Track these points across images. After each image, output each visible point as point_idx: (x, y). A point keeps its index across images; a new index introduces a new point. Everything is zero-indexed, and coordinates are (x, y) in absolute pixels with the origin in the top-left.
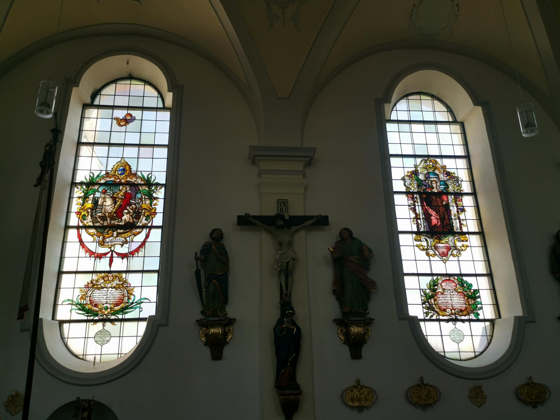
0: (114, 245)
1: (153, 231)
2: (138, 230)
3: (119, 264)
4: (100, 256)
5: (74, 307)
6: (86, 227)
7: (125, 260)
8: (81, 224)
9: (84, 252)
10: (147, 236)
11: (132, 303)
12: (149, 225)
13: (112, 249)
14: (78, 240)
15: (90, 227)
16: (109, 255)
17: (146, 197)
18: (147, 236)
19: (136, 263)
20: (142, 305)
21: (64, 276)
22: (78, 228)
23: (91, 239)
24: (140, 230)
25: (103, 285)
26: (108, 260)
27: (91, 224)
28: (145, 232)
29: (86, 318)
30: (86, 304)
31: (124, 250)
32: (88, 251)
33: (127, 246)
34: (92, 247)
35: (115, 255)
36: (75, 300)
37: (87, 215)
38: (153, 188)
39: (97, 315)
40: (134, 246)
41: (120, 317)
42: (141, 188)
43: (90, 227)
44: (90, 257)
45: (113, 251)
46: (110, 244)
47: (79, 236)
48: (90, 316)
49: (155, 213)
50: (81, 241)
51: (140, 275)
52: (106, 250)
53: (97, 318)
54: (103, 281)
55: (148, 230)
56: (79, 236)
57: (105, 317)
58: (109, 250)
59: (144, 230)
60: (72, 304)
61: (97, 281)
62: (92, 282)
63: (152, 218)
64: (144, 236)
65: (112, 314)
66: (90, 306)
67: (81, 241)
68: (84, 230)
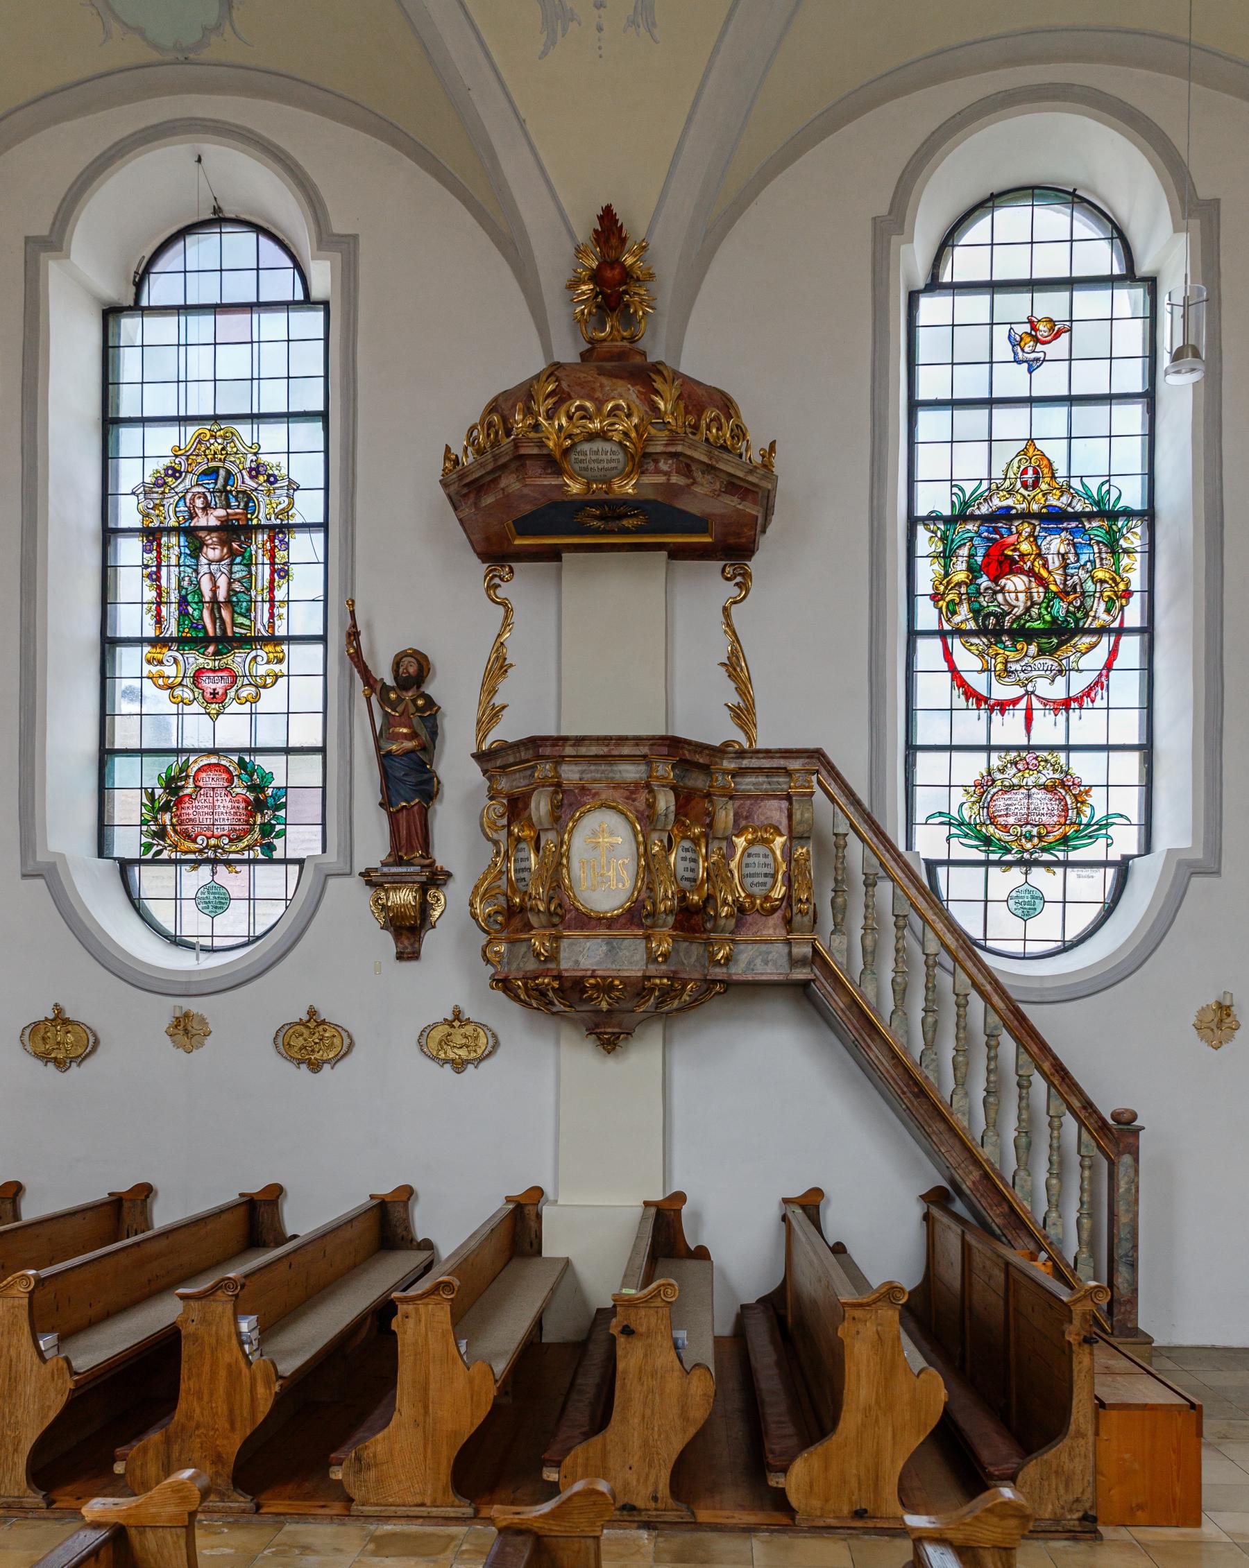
0: (1030, 680)
1: (1125, 640)
2: (1087, 640)
3: (1048, 729)
4: (1003, 706)
5: (954, 830)
6: (958, 632)
7: (1062, 717)
8: (947, 627)
9: (963, 697)
10: (1113, 653)
11: (1088, 825)
12: (1116, 625)
13: (1030, 688)
14: (945, 666)
15: (971, 633)
16: (1023, 704)
17: (1104, 549)
18: (1113, 653)
19: (1087, 726)
20: (1111, 831)
21: (921, 757)
22: (942, 634)
23: (977, 664)
24: (1094, 639)
25: (1015, 781)
26: (1021, 715)
27: (971, 625)
28: (1106, 643)
29: (982, 856)
30: (983, 824)
31: (1057, 691)
32: (969, 693)
33: (1060, 680)
34: (978, 682)
35: (1036, 704)
36: (954, 813)
37: (957, 600)
38: (1120, 524)
39: (1009, 851)
40: (1079, 683)
41: (1061, 856)
42: (1087, 525)
43: (971, 633)
44: (978, 709)
45: (1033, 693)
46: (1022, 675)
47: (948, 655)
48: (993, 852)
49: (1128, 594)
50: (953, 669)
51: (1104, 755)
52: (1017, 691)
53: (1008, 857)
54: (1014, 770)
55: (1112, 639)
56: (948, 655)
57: (1026, 856)
58: (1022, 691)
59: (1105, 639)
60: (950, 824)
61: (1002, 770)
62: (989, 774)
63: (1122, 608)
64: (1106, 656)
65: (1043, 850)
66: (991, 829)
67: (953, 669)
68: (957, 642)
